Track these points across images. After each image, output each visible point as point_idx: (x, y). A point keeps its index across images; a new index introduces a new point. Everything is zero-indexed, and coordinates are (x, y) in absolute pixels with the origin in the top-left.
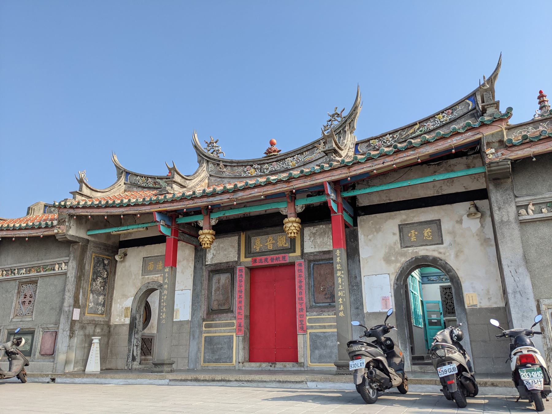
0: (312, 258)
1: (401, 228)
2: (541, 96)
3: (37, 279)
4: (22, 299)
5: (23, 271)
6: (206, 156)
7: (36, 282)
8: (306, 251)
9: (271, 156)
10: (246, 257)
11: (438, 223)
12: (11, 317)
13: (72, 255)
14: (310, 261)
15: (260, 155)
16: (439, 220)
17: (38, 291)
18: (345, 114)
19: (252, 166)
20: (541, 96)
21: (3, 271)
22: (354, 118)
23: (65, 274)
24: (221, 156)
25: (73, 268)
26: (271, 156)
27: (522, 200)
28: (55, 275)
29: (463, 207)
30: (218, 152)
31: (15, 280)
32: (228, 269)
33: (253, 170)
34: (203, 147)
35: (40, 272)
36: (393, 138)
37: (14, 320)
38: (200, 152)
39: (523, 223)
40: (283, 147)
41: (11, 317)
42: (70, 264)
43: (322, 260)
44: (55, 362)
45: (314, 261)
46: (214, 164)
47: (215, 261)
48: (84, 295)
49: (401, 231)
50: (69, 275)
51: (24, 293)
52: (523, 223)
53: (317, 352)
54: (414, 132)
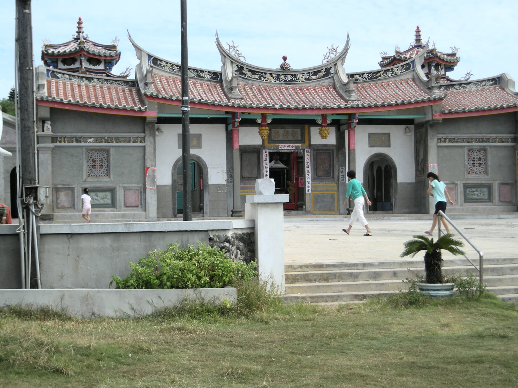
0: (316, 148)
1: (370, 135)
2: (418, 31)
3: (108, 148)
4: (91, 163)
5: (92, 140)
6: (229, 57)
7: (107, 151)
8: (312, 143)
9: (284, 68)
10: (268, 143)
11: (388, 135)
12: (84, 177)
13: (147, 132)
14: (314, 150)
15: (275, 65)
16: (389, 134)
17: (111, 158)
18: (340, 50)
19: (271, 74)
20: (418, 31)
21: (64, 138)
22: (346, 56)
23: (144, 147)
24: (242, 60)
25: (151, 142)
26: (284, 68)
27: (440, 136)
28: (129, 147)
29: (401, 128)
30: (239, 55)
31: (81, 147)
32: (256, 151)
33: (272, 78)
34: (226, 47)
35: (113, 142)
36: (368, 76)
37: (88, 180)
38: (224, 51)
39: (439, 147)
40: (294, 65)
41: (84, 177)
42: (147, 139)
43: (322, 150)
44: (147, 211)
45: (317, 150)
46: (238, 66)
49: (369, 137)
50: (147, 147)
51: (92, 158)
52: (439, 147)
53: (318, 205)
54: (380, 76)
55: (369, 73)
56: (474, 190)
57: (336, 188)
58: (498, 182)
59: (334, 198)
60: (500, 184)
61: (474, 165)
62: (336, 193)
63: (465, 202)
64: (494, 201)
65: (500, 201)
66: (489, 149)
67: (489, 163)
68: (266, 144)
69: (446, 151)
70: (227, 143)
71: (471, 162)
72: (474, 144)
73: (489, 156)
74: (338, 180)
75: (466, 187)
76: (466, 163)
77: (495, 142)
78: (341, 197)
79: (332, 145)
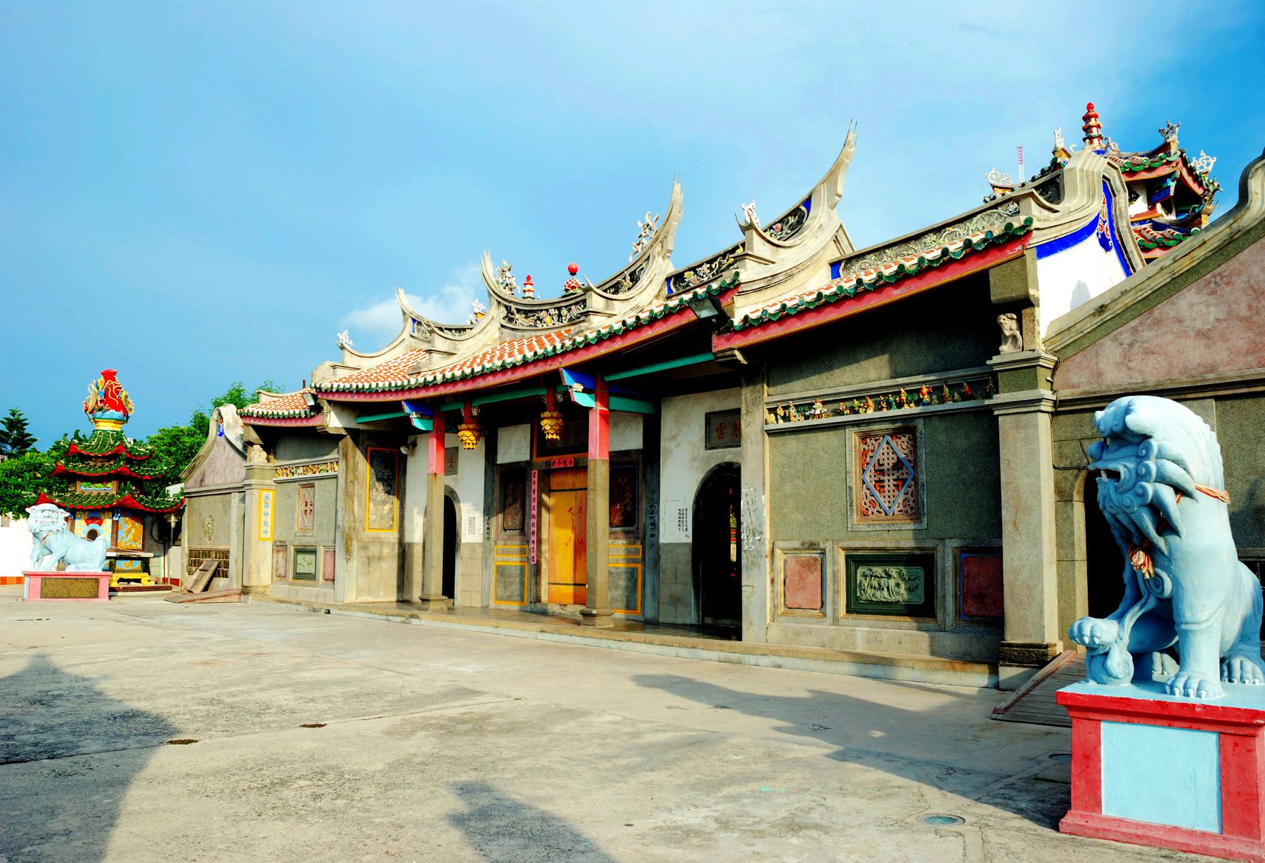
5: (301, 470)
36: (711, 269)
47: (507, 461)
48: (360, 505)
55: (711, 262)
56: (878, 570)
57: (640, 556)
58: (955, 543)
59: (636, 581)
60: (963, 550)
61: (880, 484)
62: (639, 566)
63: (849, 610)
64: (939, 615)
65: (959, 613)
66: (920, 424)
67: (923, 478)
68: (535, 459)
69: (792, 442)
70: (487, 459)
71: (870, 478)
72: (871, 413)
73: (922, 452)
74: (644, 537)
75: (855, 560)
76: (854, 481)
77: (900, 405)
78: (648, 578)
79: (637, 451)
